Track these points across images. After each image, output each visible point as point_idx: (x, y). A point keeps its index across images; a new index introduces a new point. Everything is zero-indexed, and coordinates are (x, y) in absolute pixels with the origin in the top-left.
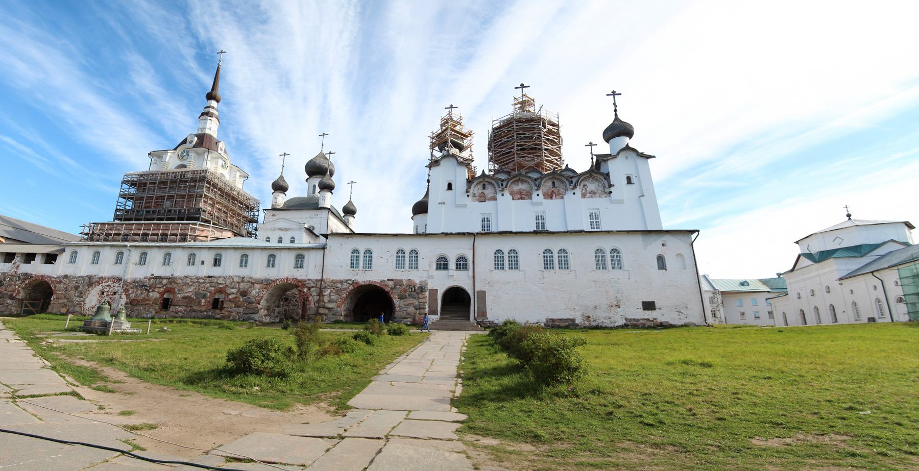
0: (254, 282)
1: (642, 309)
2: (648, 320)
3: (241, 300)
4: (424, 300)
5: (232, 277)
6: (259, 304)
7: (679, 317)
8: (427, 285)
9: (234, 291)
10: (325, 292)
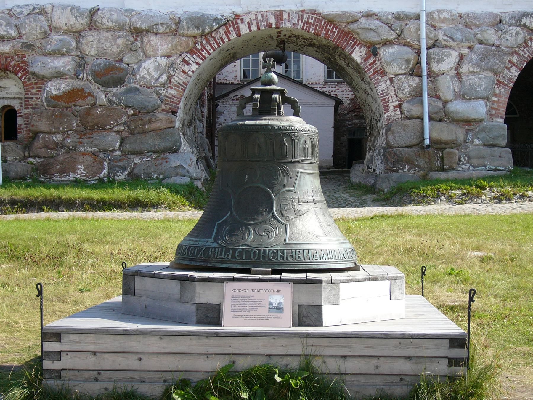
0: (144, 27)
5: (42, 11)
10: (440, 61)
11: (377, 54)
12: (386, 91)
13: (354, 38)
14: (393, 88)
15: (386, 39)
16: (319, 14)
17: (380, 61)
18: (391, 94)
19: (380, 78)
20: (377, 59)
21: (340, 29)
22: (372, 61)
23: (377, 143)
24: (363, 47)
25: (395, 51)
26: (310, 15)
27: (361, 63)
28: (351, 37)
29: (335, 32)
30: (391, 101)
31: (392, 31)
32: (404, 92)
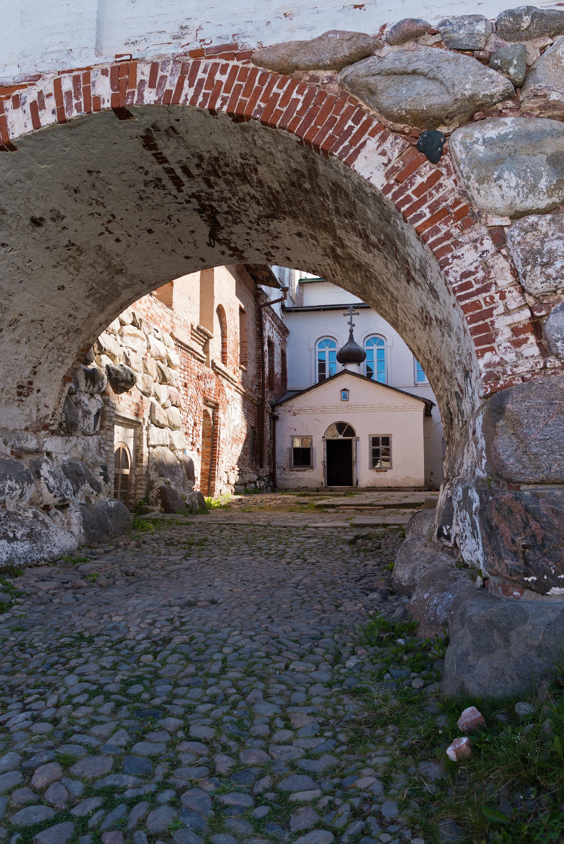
11: (442, 153)
12: (480, 274)
13: (361, 113)
14: (505, 264)
15: (472, 98)
16: (247, 55)
17: (453, 177)
18: (500, 283)
19: (455, 232)
20: (444, 171)
21: (312, 91)
22: (425, 179)
23: (462, 464)
24: (391, 138)
25: (506, 134)
26: (217, 60)
27: (387, 189)
28: (351, 109)
29: (297, 101)
30: (501, 309)
31: (491, 71)
32: (551, 271)
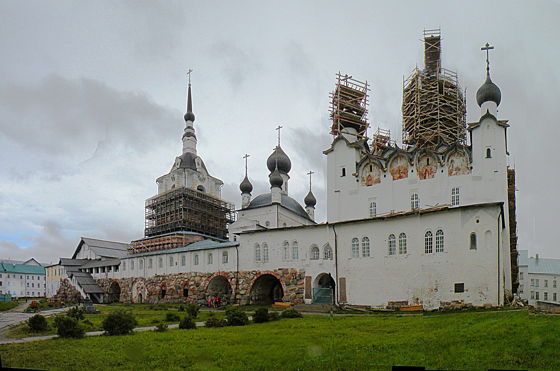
1: (454, 291)
2: (457, 302)
3: (196, 289)
4: (301, 286)
6: (206, 292)
7: (480, 298)
8: (304, 273)
9: (192, 283)
